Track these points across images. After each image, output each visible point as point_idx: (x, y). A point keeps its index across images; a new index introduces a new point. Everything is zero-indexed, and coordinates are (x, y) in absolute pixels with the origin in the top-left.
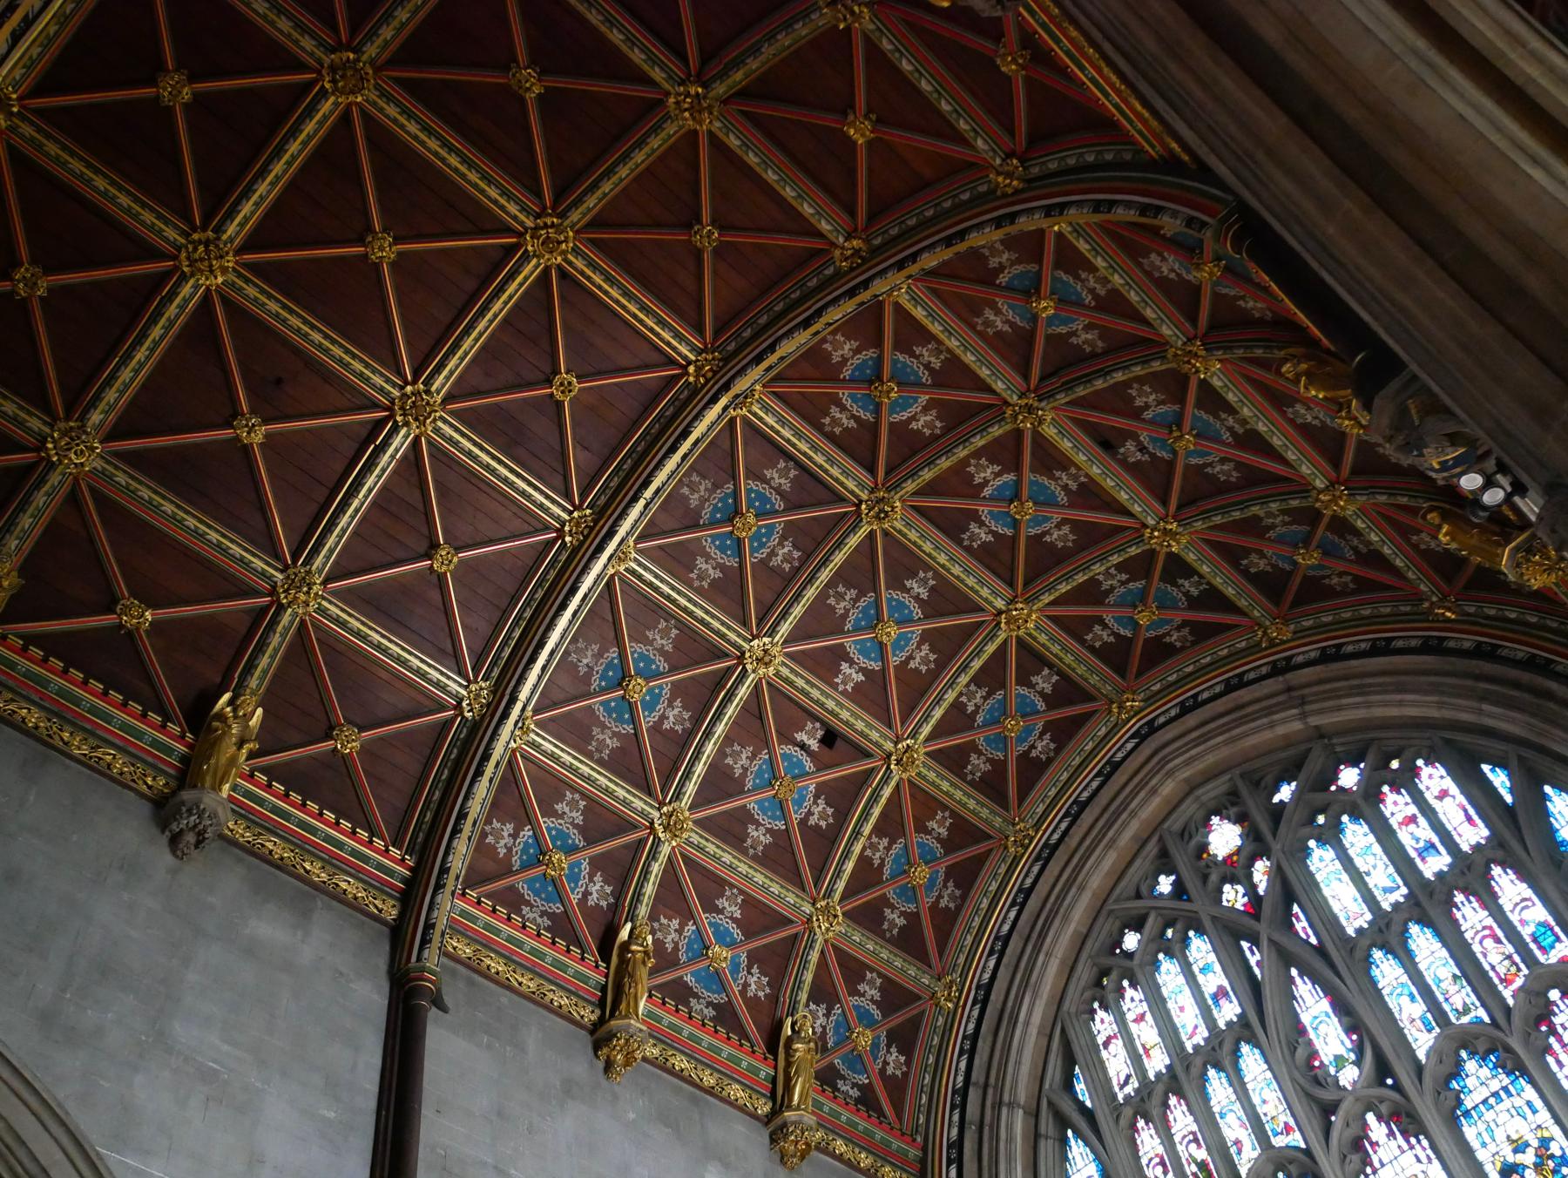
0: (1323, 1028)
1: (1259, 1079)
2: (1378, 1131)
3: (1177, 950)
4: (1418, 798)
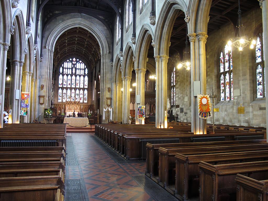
3: (70, 63)
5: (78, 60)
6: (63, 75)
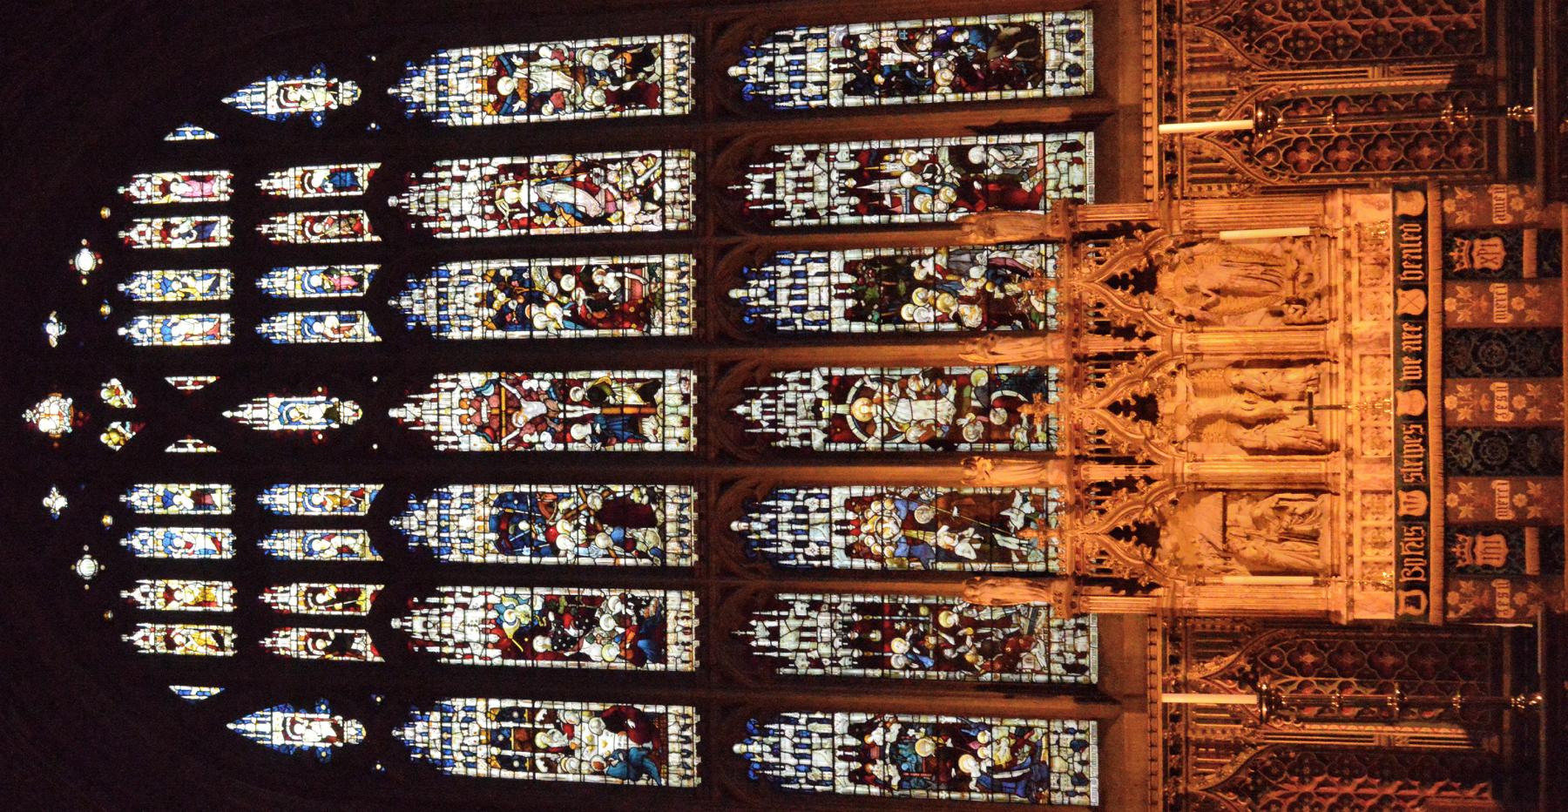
0: (293, 414)
1: (300, 500)
2: (407, 413)
3: (131, 520)
4: (152, 211)
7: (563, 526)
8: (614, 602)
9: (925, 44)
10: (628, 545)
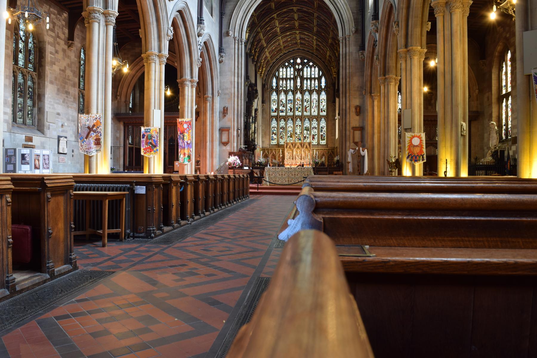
2: (299, 92)
3: (290, 68)
5: (306, 61)
6: (278, 93)
7: (290, 105)
8: (285, 109)
9: (324, 132)
10: (289, 110)
